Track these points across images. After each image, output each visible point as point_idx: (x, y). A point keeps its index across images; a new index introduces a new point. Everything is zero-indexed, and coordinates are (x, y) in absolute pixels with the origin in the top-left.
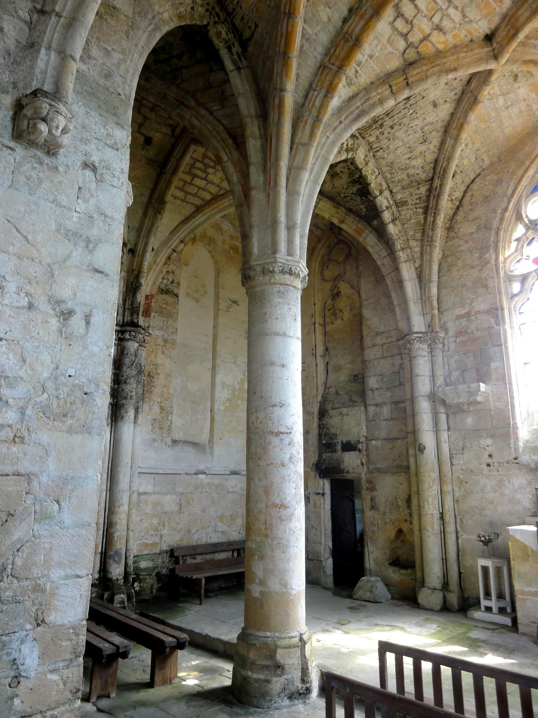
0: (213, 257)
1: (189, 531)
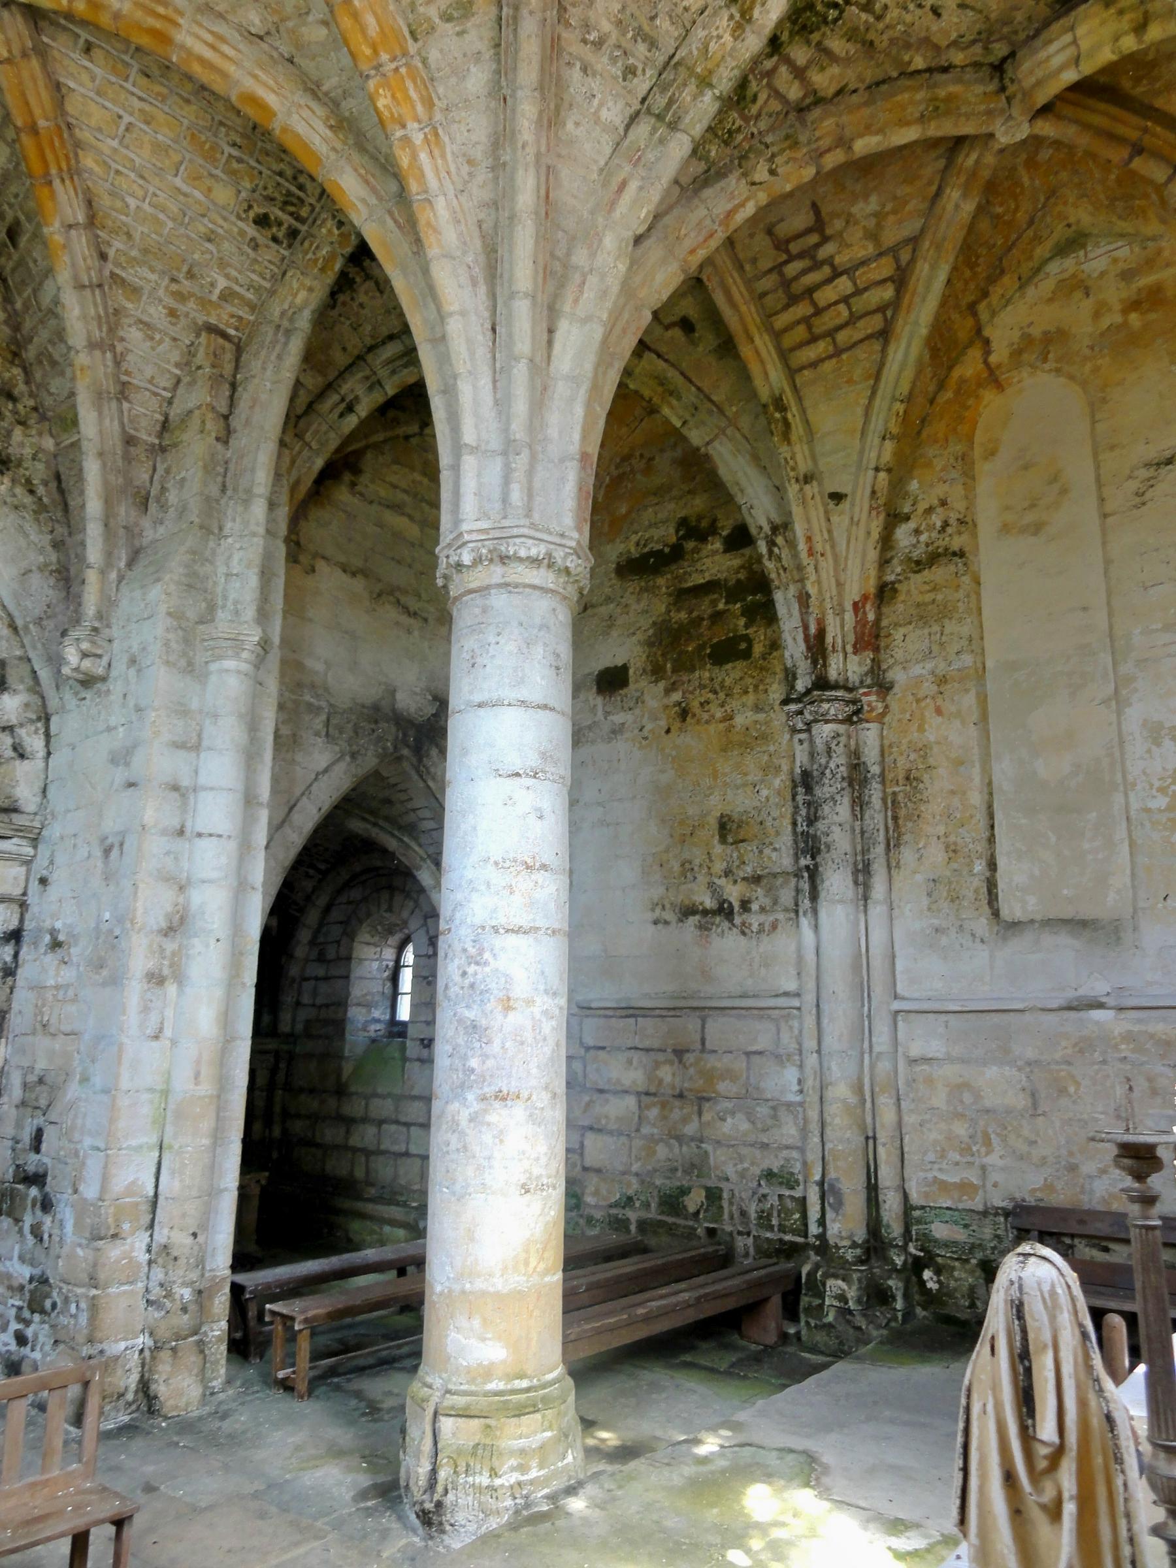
0: (1071, 378)
1: (1073, 1168)
